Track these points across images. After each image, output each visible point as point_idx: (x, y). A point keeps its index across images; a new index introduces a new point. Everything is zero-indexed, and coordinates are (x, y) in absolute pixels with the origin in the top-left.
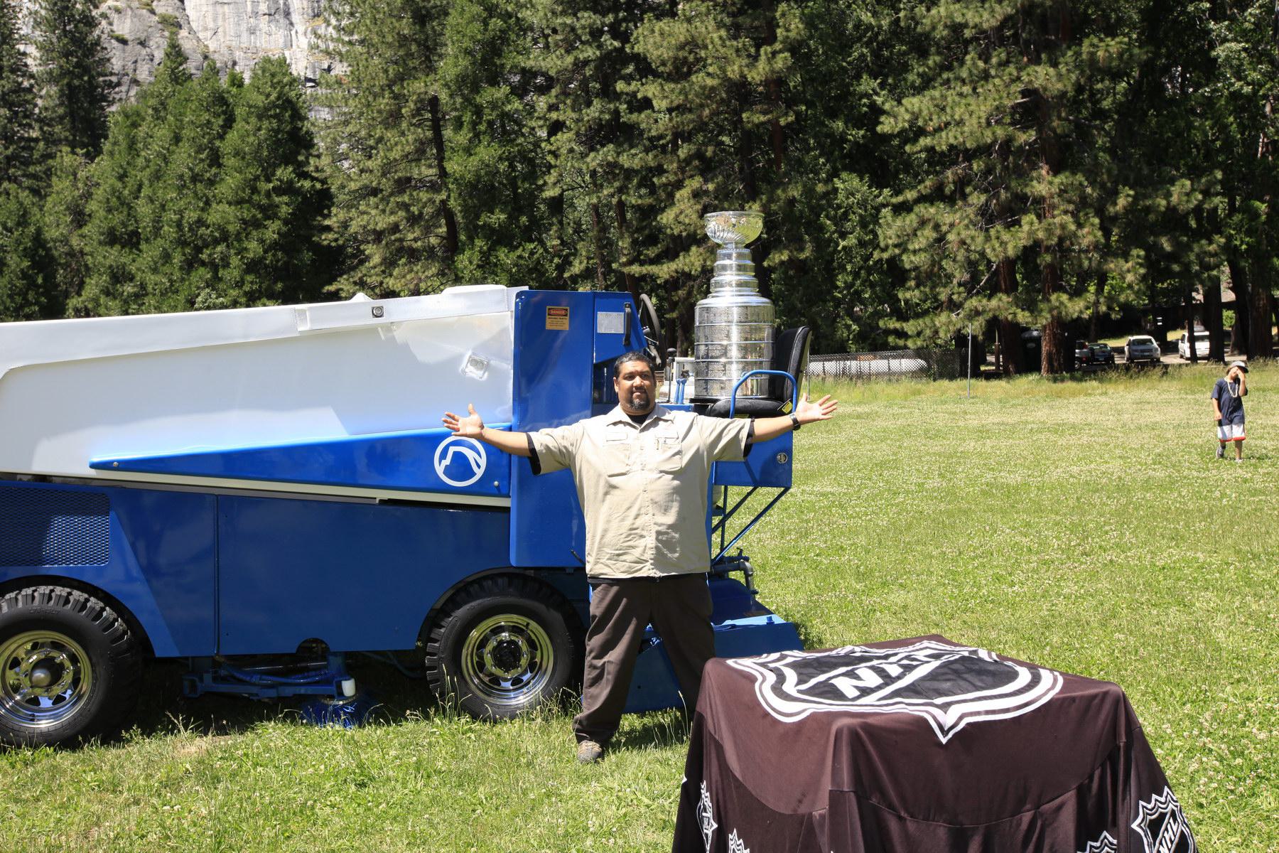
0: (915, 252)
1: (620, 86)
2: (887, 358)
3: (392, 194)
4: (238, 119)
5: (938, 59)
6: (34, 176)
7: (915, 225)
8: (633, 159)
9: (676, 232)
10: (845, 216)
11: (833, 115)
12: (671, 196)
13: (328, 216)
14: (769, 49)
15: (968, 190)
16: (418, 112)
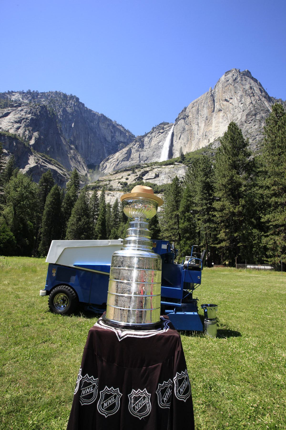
0: (270, 245)
1: (210, 213)
2: (264, 266)
5: (273, 208)
6: (117, 227)
8: (212, 225)
10: (254, 237)
11: (252, 218)
12: (220, 232)
13: (160, 234)
14: (238, 206)
15: (281, 233)
16: (175, 217)
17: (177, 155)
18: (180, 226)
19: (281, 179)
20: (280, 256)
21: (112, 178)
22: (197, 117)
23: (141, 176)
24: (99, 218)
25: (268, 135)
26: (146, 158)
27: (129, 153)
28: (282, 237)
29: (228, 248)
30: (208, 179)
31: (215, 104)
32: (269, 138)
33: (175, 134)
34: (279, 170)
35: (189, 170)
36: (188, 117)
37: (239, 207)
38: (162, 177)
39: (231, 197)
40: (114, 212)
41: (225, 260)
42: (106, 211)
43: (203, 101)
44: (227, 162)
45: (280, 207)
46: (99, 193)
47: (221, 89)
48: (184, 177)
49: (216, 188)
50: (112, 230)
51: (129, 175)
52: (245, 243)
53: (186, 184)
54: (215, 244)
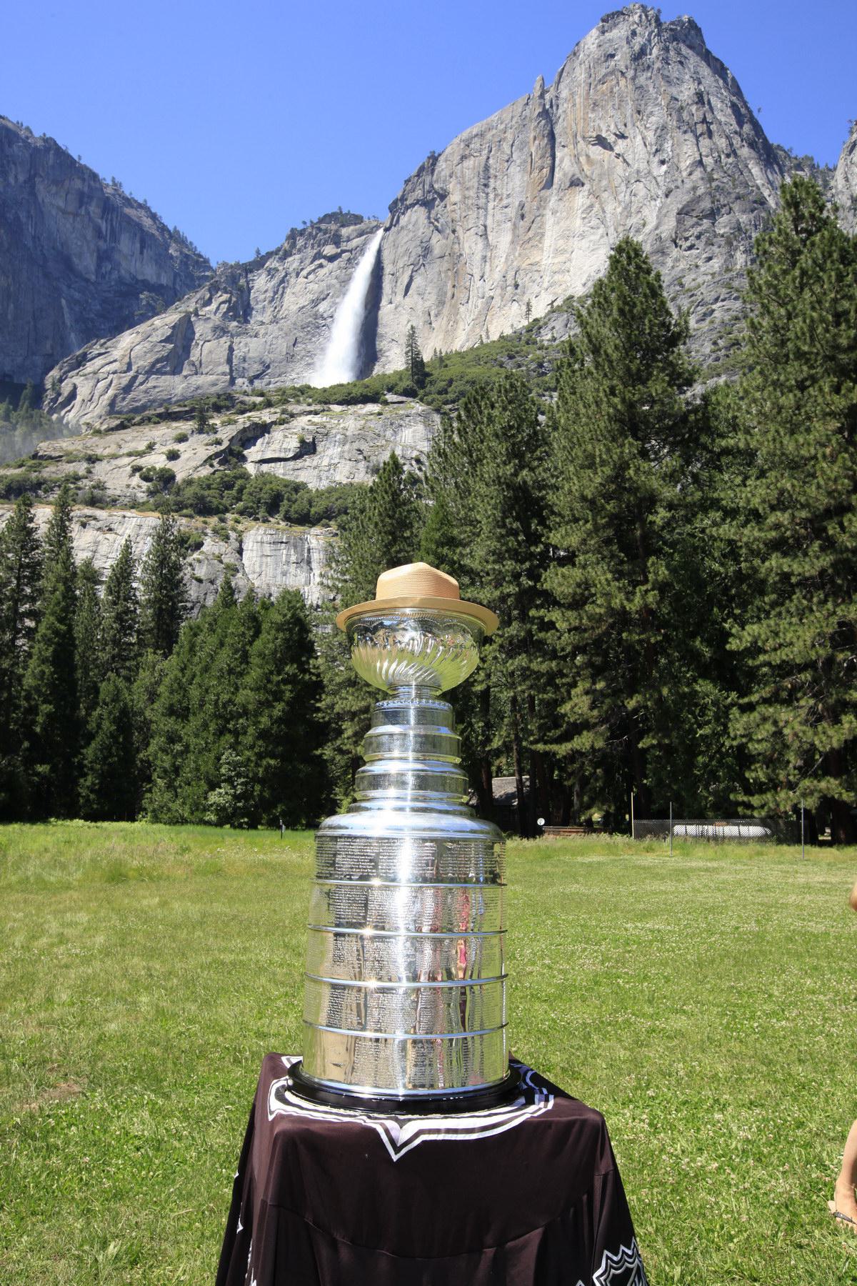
0: (759, 741)
1: (533, 613)
2: (738, 825)
4: (264, 631)
5: (774, 596)
6: (129, 669)
9: (572, 720)
10: (703, 714)
11: (693, 636)
12: (569, 693)
13: (320, 701)
14: (644, 588)
15: (799, 695)
17: (394, 361)
19: (805, 483)
20: (797, 784)
21: (102, 446)
22: (482, 202)
23: (236, 448)
24: (42, 629)
25: (763, 305)
26: (260, 368)
27: (183, 337)
28: (803, 713)
29: (600, 759)
30: (525, 472)
31: (558, 155)
32: (767, 318)
33: (388, 268)
34: (798, 447)
35: (445, 431)
36: (443, 196)
37: (647, 591)
38: (330, 452)
39: (615, 547)
40: (115, 603)
41: (589, 807)
42: (75, 598)
43: (509, 136)
44: (604, 406)
45: (797, 590)
46: (43, 515)
47: (581, 91)
48: (423, 459)
49: (556, 509)
50: (103, 686)
51: (182, 439)
52: (668, 736)
53: (432, 488)
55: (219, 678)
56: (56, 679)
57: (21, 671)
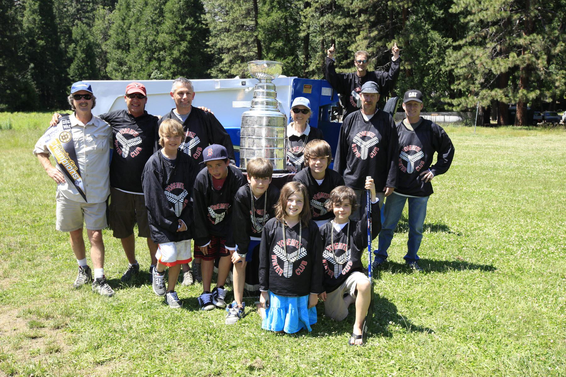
0: (461, 68)
2: (444, 115)
3: (235, 32)
7: (462, 56)
10: (431, 52)
13: (208, 41)
18: (261, 21)
28: (488, 51)
54: (343, 67)
55: (146, 26)
56: (44, 24)
57: (19, 18)
